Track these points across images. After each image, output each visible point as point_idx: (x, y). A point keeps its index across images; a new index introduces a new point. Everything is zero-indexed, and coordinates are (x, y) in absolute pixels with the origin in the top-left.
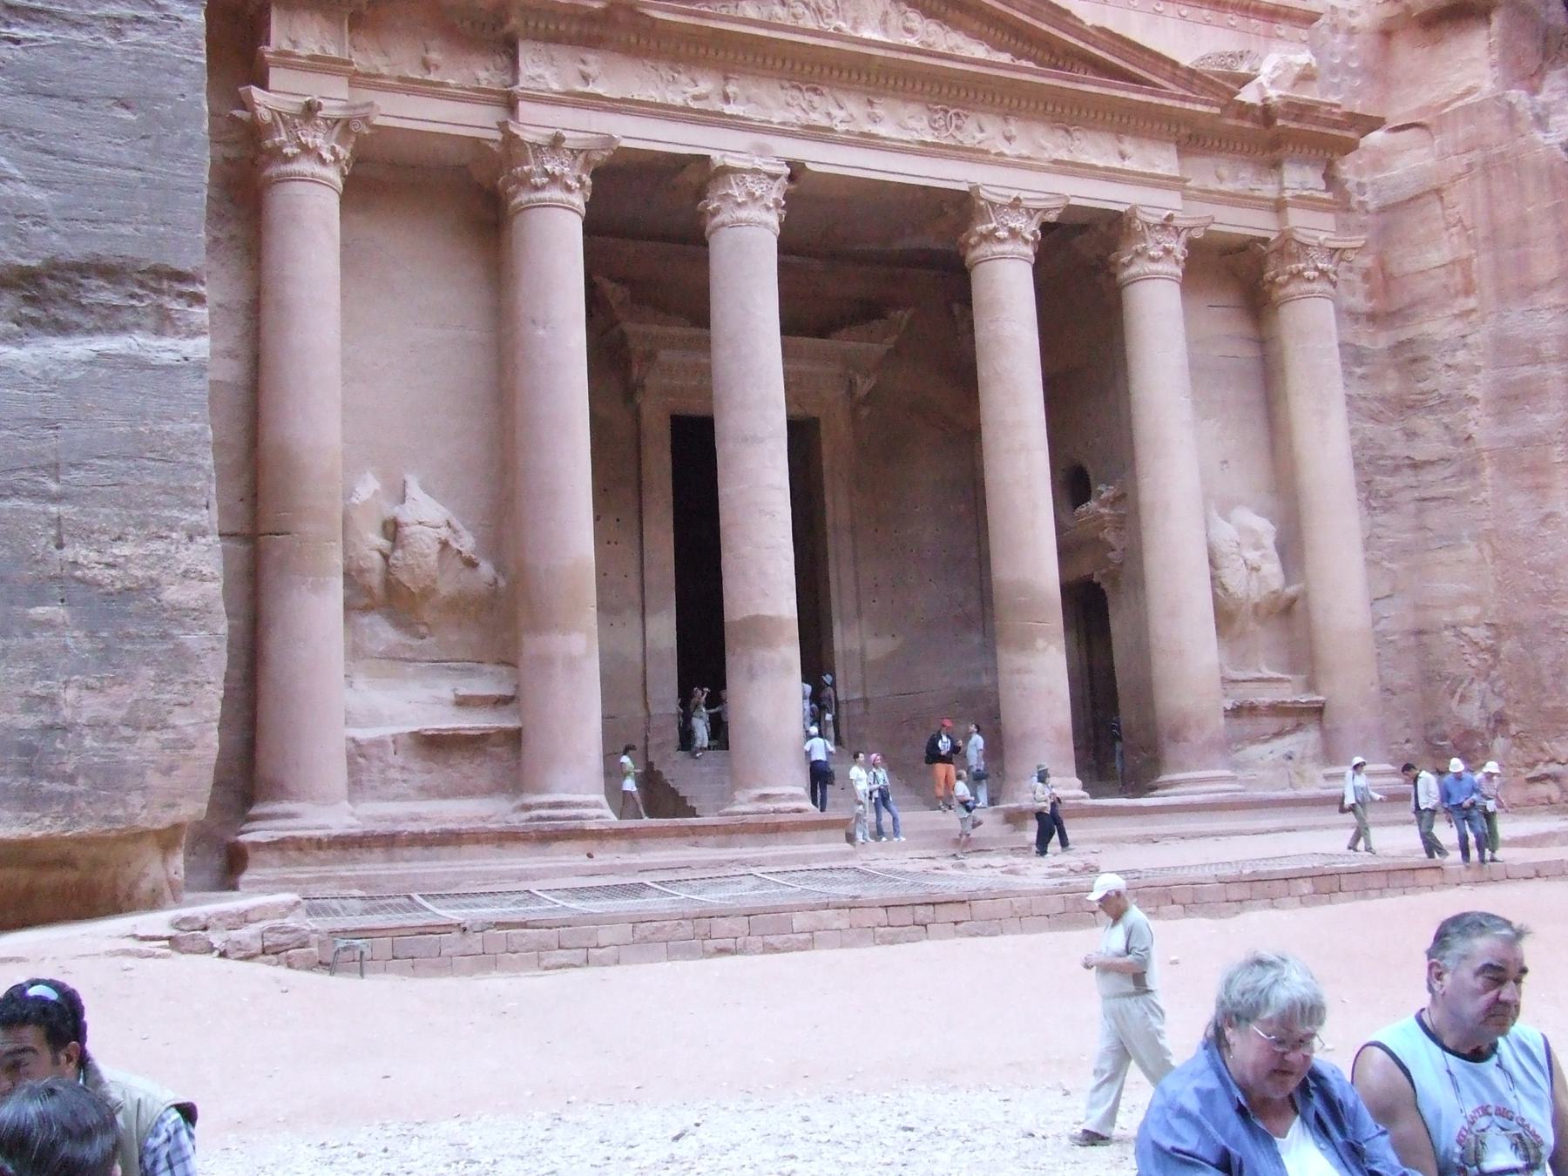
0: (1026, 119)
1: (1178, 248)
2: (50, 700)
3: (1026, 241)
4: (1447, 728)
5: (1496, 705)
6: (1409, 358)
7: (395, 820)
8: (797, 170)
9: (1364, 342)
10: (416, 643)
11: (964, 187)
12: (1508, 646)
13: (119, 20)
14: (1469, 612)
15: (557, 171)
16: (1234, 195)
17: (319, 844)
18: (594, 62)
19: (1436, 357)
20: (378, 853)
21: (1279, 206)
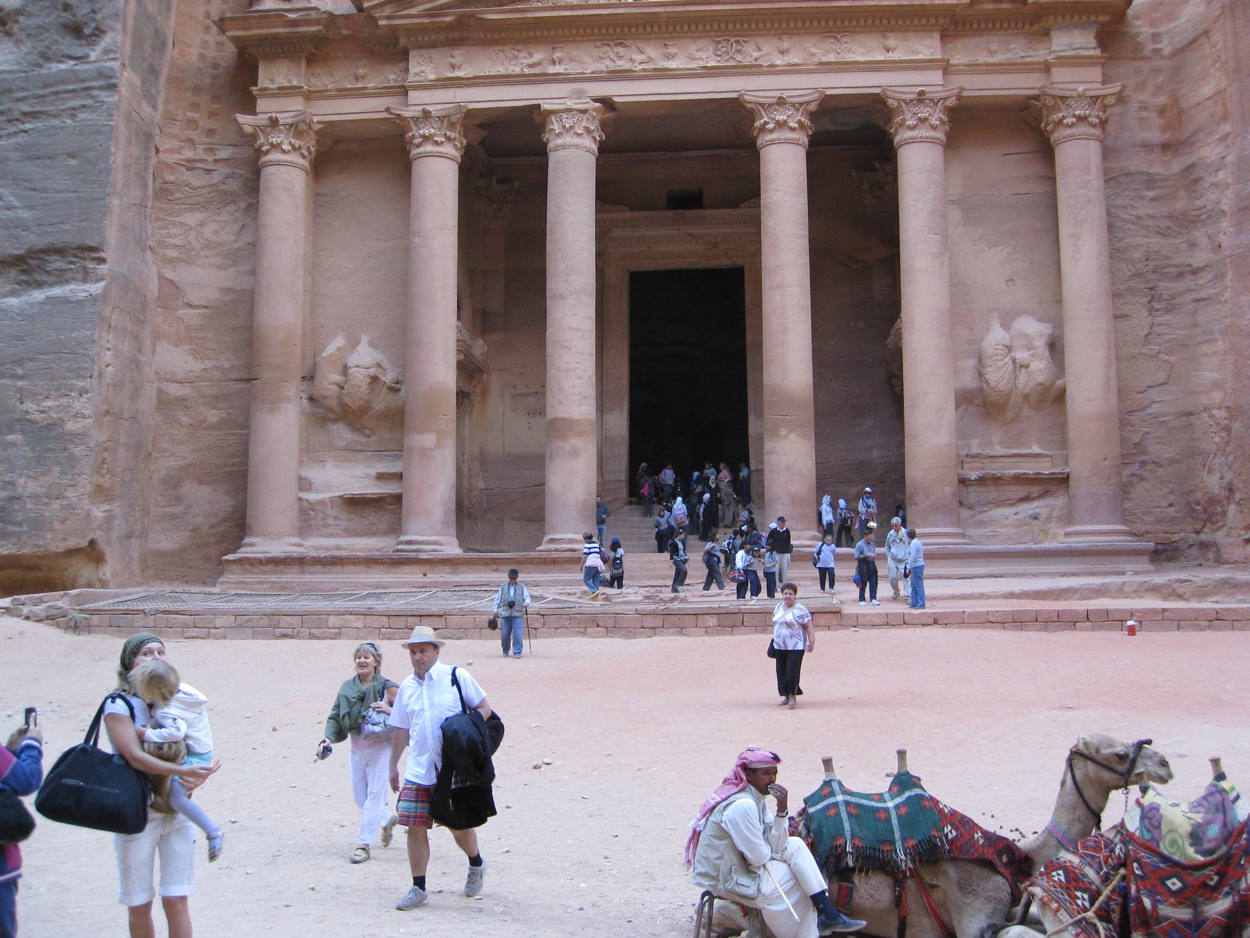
0: (798, 35)
1: (936, 116)
2: (12, 483)
3: (793, 130)
4: (1199, 495)
5: (1229, 476)
6: (1191, 179)
7: (327, 549)
8: (607, 103)
9: (1157, 169)
10: (364, 440)
11: (734, 95)
12: (1236, 426)
13: (74, 109)
14: (1217, 396)
15: (427, 132)
16: (1002, 64)
17: (260, 562)
18: (458, 55)
19: (1206, 177)
20: (296, 569)
21: (1046, 68)
